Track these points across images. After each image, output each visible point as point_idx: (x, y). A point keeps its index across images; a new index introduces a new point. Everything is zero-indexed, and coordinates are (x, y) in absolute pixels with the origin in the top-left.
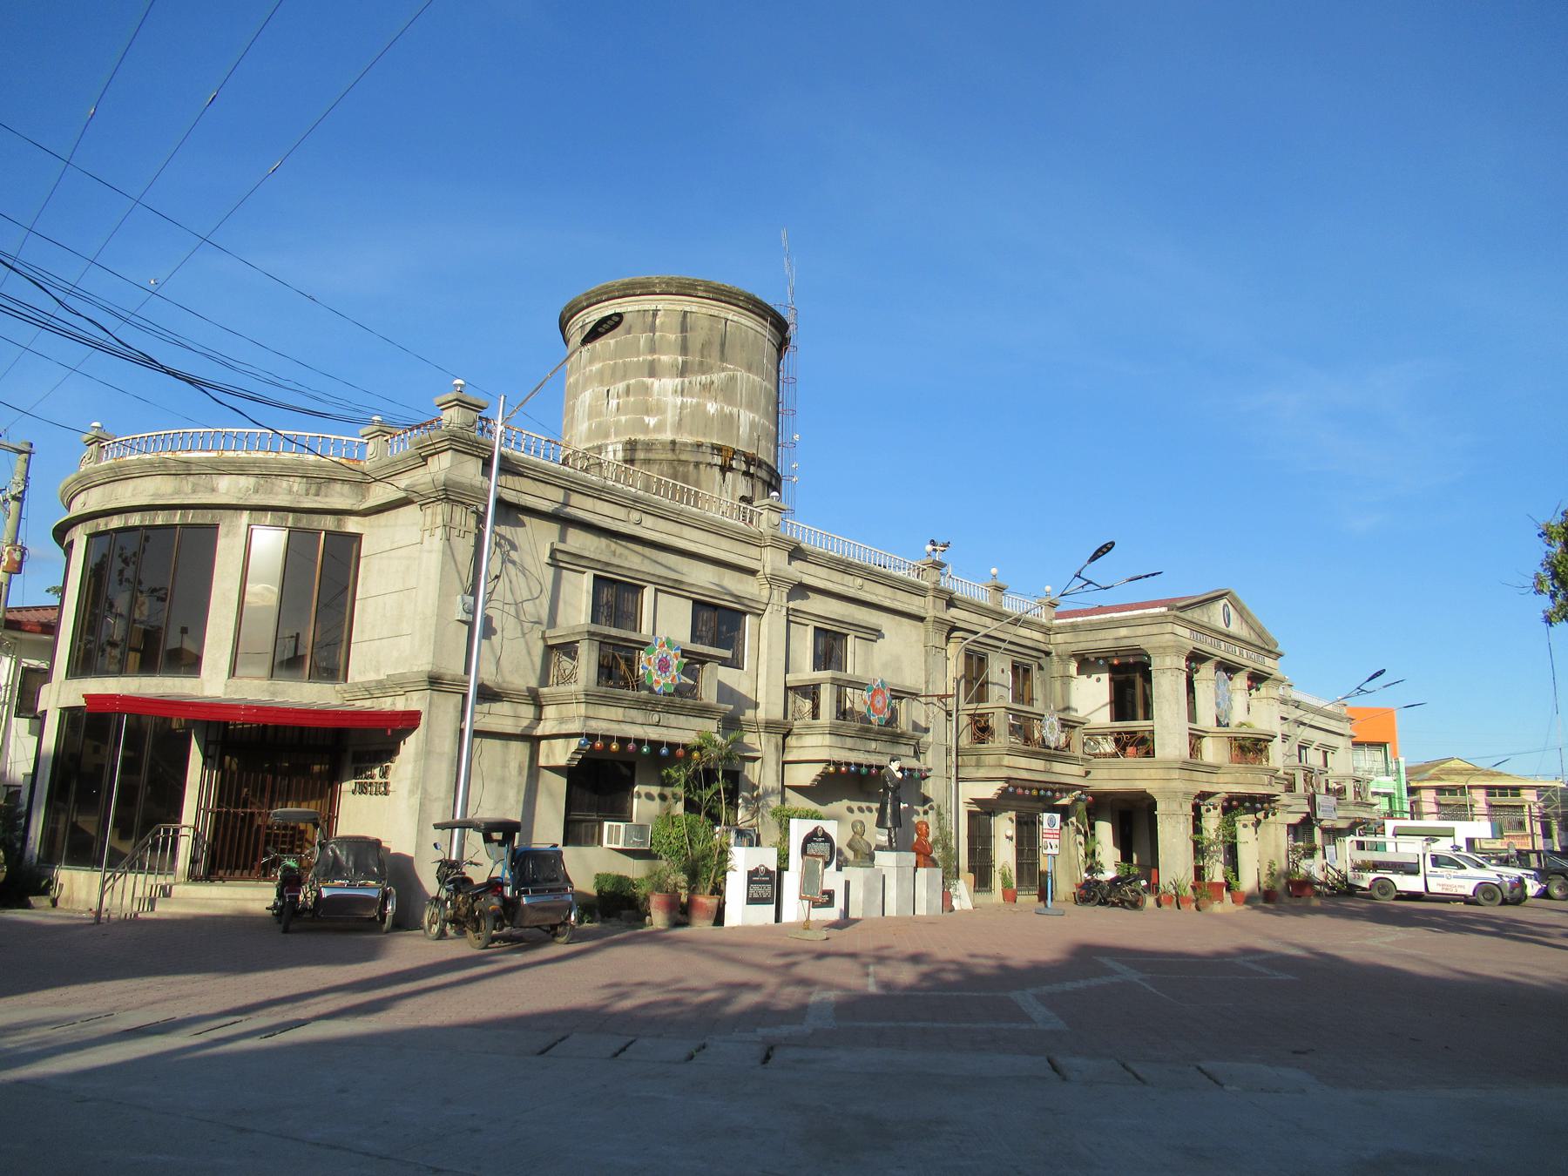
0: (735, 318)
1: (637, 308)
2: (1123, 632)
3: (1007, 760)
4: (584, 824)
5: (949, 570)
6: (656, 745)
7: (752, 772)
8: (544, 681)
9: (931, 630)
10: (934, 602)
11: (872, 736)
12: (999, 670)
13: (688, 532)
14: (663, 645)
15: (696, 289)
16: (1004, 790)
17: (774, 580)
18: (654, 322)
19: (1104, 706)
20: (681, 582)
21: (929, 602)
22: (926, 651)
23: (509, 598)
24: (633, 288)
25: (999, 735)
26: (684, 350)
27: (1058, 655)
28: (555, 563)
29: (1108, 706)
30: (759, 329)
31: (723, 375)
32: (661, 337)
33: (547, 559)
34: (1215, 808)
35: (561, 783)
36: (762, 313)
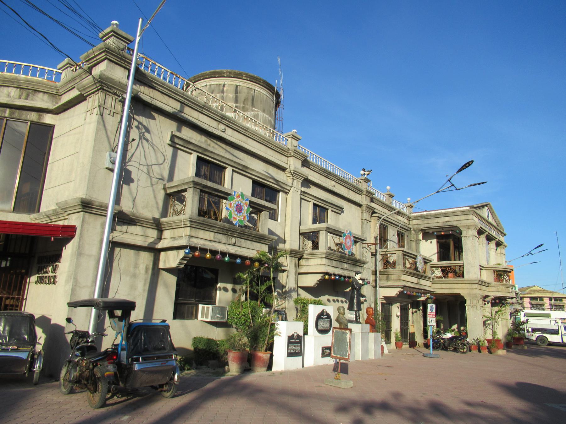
0: (259, 90)
1: (216, 83)
2: (447, 219)
3: (404, 277)
4: (187, 306)
5: (371, 183)
6: (233, 256)
7: (282, 278)
8: (164, 213)
9: (365, 211)
10: (366, 198)
11: (345, 260)
12: (392, 233)
13: (250, 141)
14: (238, 197)
15: (242, 76)
16: (401, 293)
17: (295, 174)
18: (223, 89)
19: (434, 254)
20: (247, 168)
21: (363, 197)
22: (362, 222)
23: (143, 161)
24: (215, 74)
25: (399, 264)
26: (236, 101)
27: (414, 230)
28: (174, 145)
29: (436, 255)
30: (268, 95)
31: (253, 113)
32: (227, 96)
33: (168, 141)
34: (488, 303)
35: (172, 280)
36: (269, 88)
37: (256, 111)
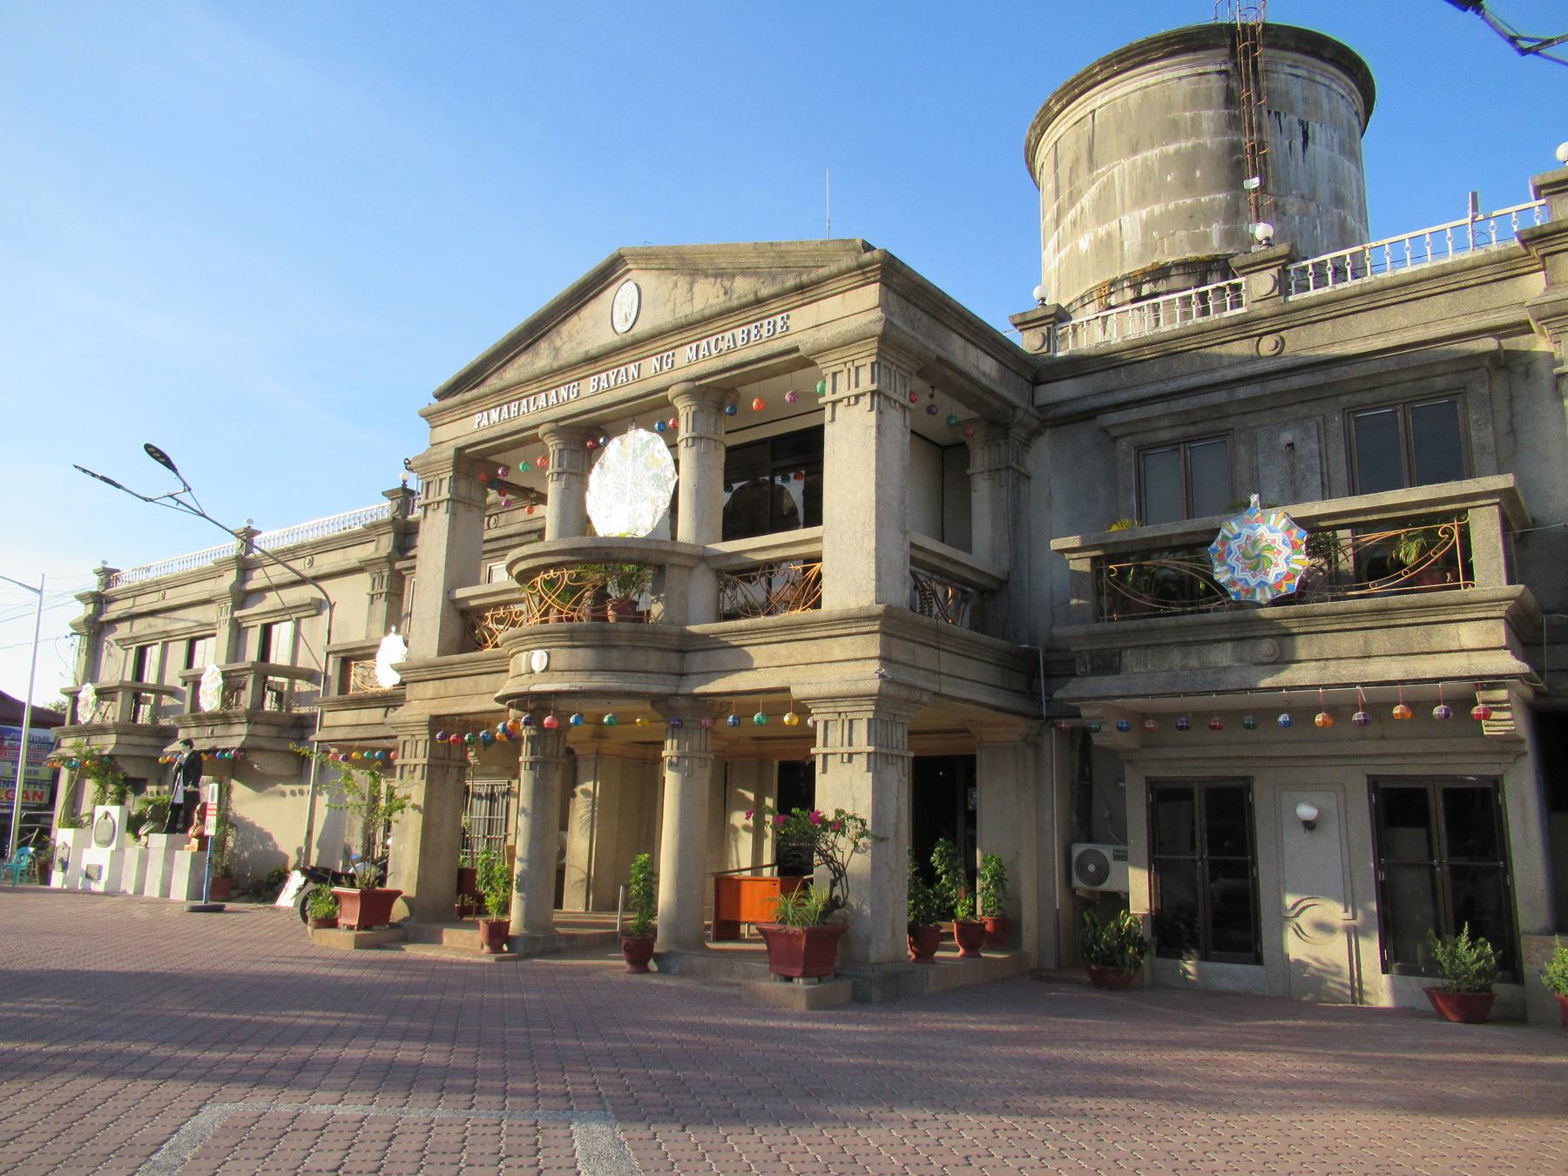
37: (1104, 174)
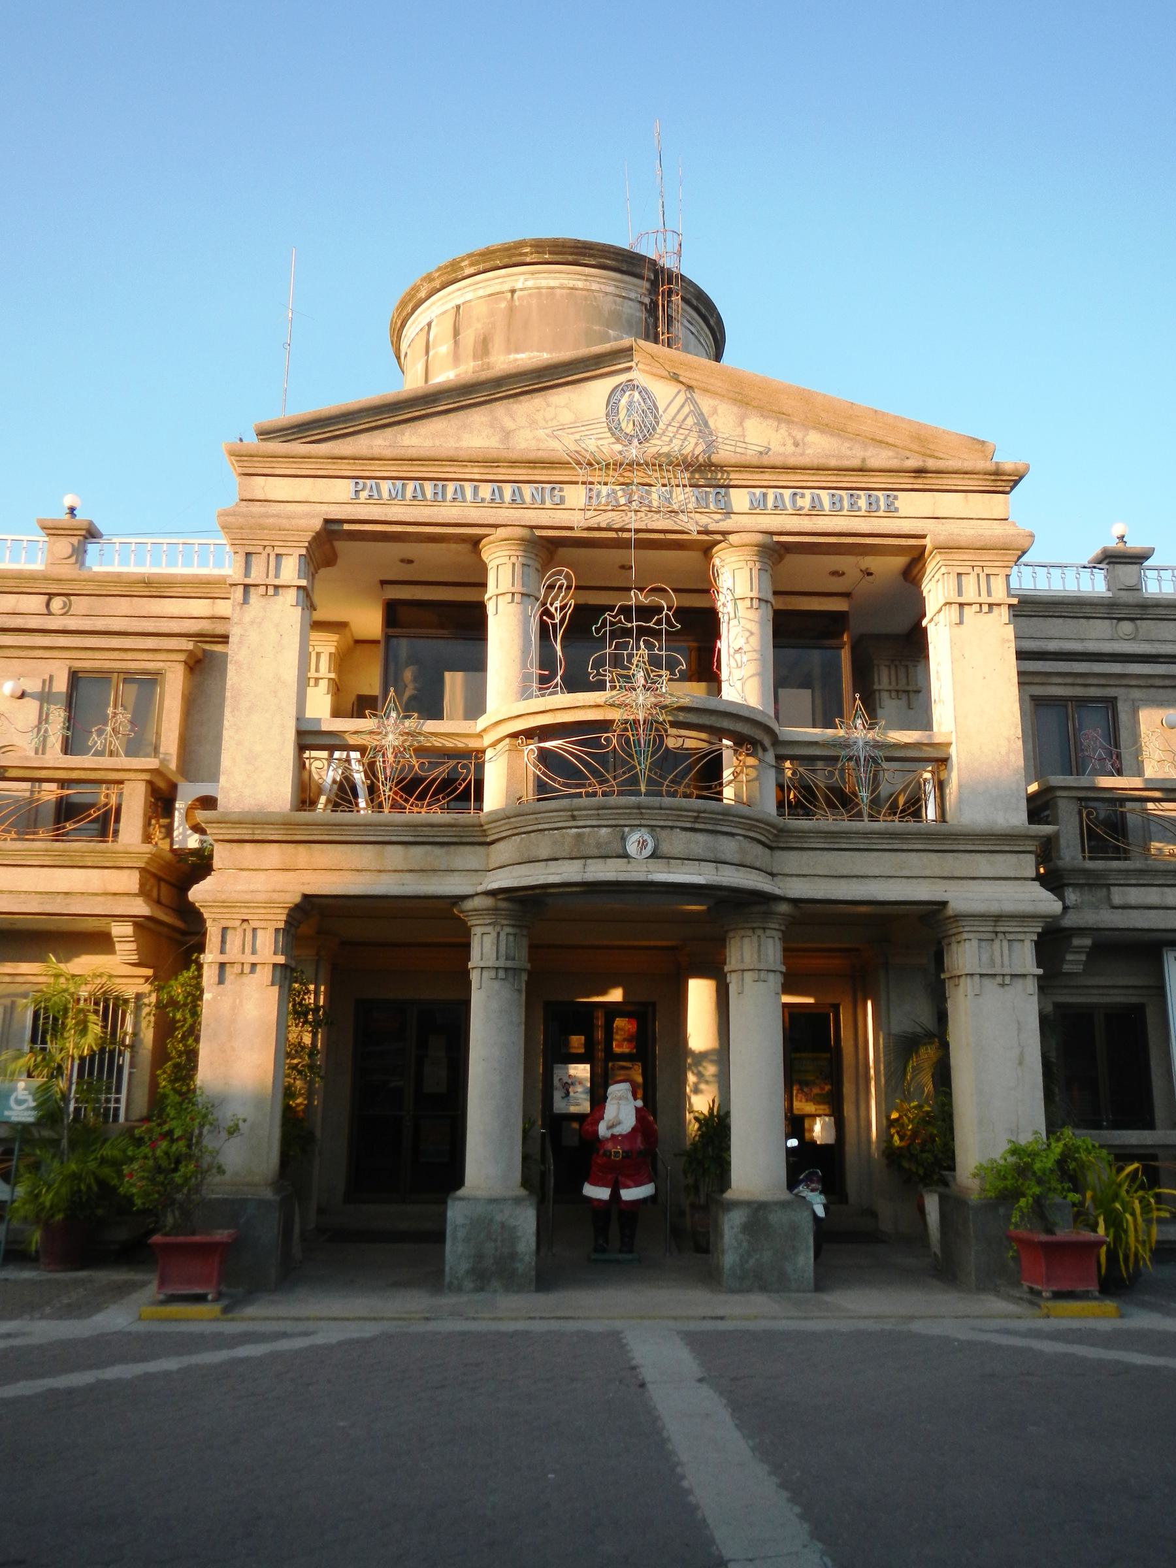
0: (530, 284)
36: (570, 258)
